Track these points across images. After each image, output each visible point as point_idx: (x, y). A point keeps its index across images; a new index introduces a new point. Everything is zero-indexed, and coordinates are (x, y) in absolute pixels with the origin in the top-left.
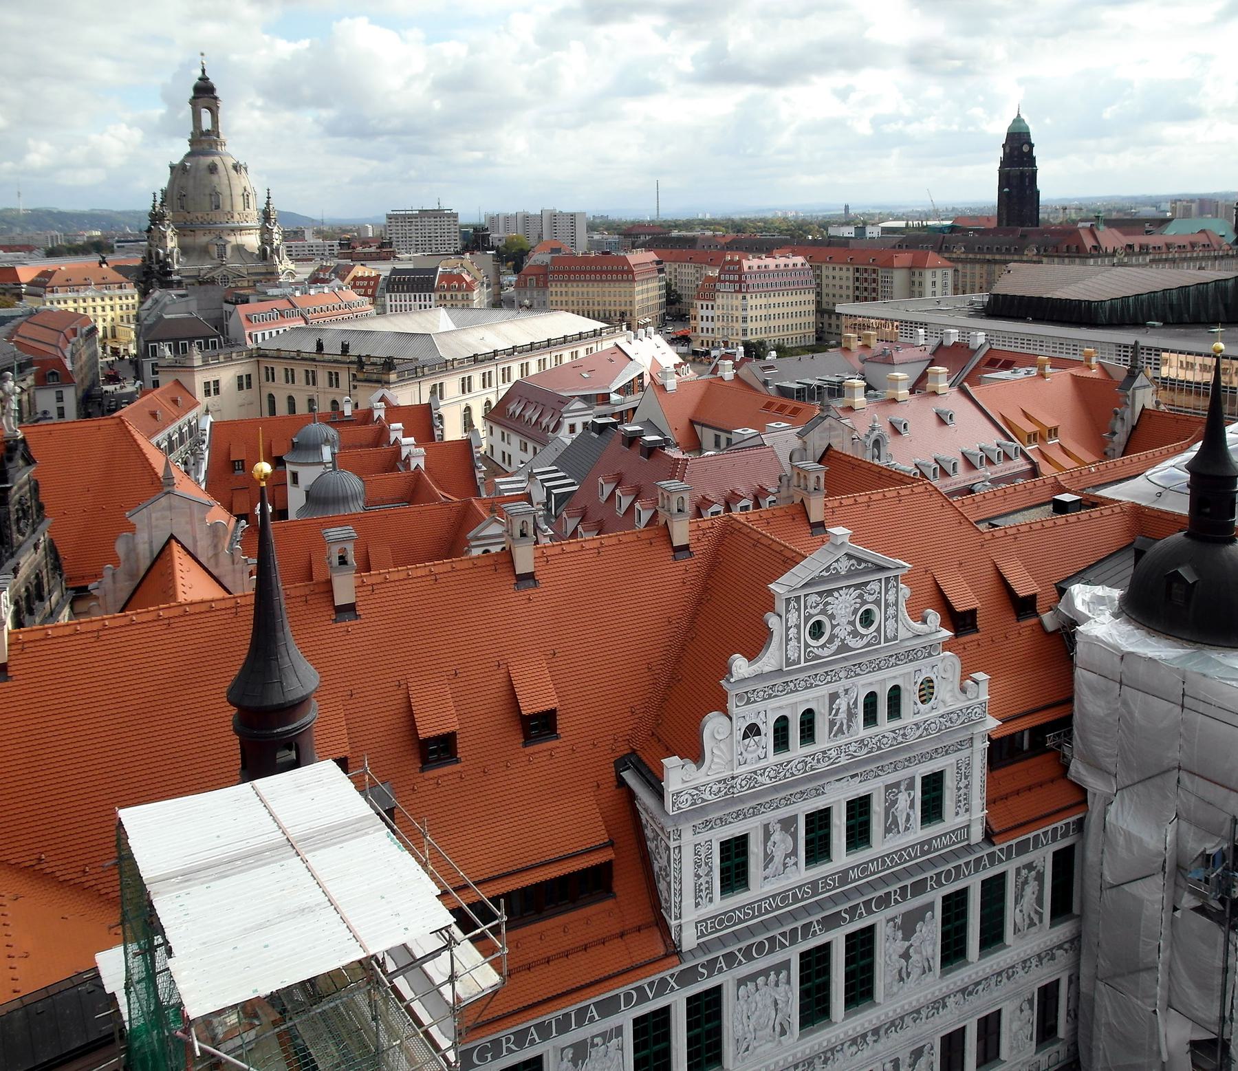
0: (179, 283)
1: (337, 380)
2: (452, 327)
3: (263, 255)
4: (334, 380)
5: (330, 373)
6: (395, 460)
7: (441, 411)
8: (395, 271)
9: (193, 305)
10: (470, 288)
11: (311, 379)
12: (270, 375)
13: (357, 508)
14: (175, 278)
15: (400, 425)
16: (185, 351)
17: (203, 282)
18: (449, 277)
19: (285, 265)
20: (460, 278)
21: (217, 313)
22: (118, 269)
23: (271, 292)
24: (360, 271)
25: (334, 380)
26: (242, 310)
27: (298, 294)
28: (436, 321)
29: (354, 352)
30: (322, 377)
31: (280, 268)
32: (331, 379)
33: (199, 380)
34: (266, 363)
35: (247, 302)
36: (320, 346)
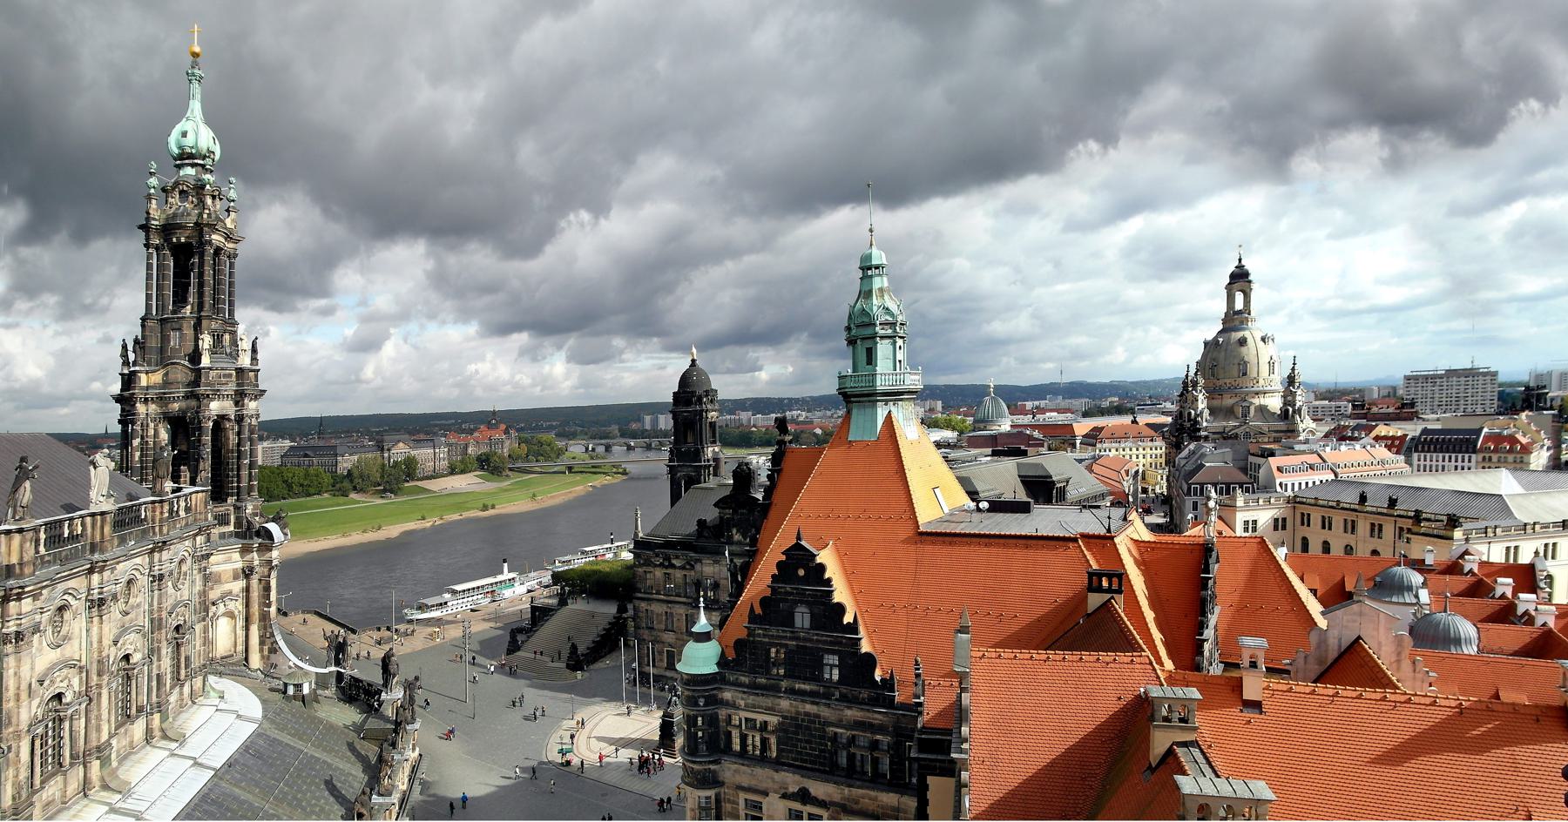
0: (1206, 438)
1: (1380, 530)
2: (1521, 490)
3: (1284, 415)
4: (1375, 530)
5: (1373, 525)
6: (1506, 613)
7: (1552, 571)
8: (1425, 431)
9: (1229, 458)
10: (1526, 450)
11: (1352, 527)
12: (1306, 520)
13: (1472, 650)
14: (1203, 433)
15: (1510, 581)
16: (1228, 493)
17: (1225, 437)
18: (1497, 438)
19: (1306, 424)
20: (1512, 440)
21: (1242, 464)
22: (1153, 426)
23: (1297, 447)
24: (1382, 430)
25: (1375, 530)
26: (1274, 462)
27: (1328, 449)
28: (1503, 482)
29: (1401, 507)
30: (1363, 527)
31: (1301, 426)
32: (1372, 530)
33: (1240, 518)
34: (1306, 510)
35: (1272, 454)
36: (1363, 499)
